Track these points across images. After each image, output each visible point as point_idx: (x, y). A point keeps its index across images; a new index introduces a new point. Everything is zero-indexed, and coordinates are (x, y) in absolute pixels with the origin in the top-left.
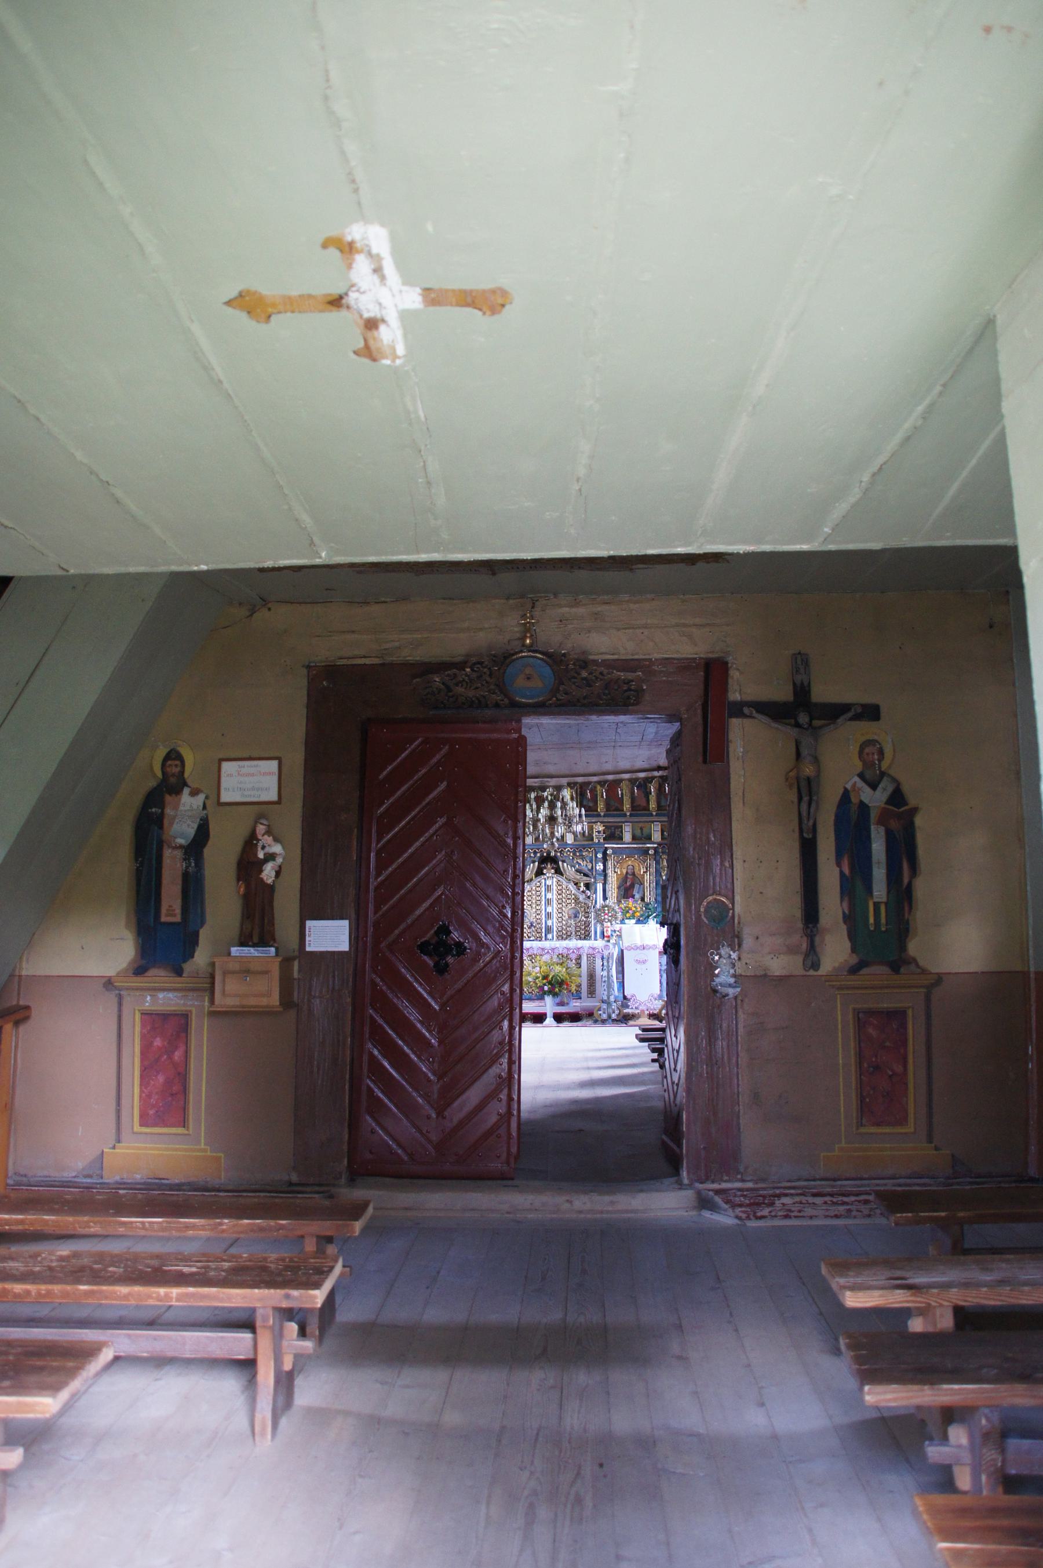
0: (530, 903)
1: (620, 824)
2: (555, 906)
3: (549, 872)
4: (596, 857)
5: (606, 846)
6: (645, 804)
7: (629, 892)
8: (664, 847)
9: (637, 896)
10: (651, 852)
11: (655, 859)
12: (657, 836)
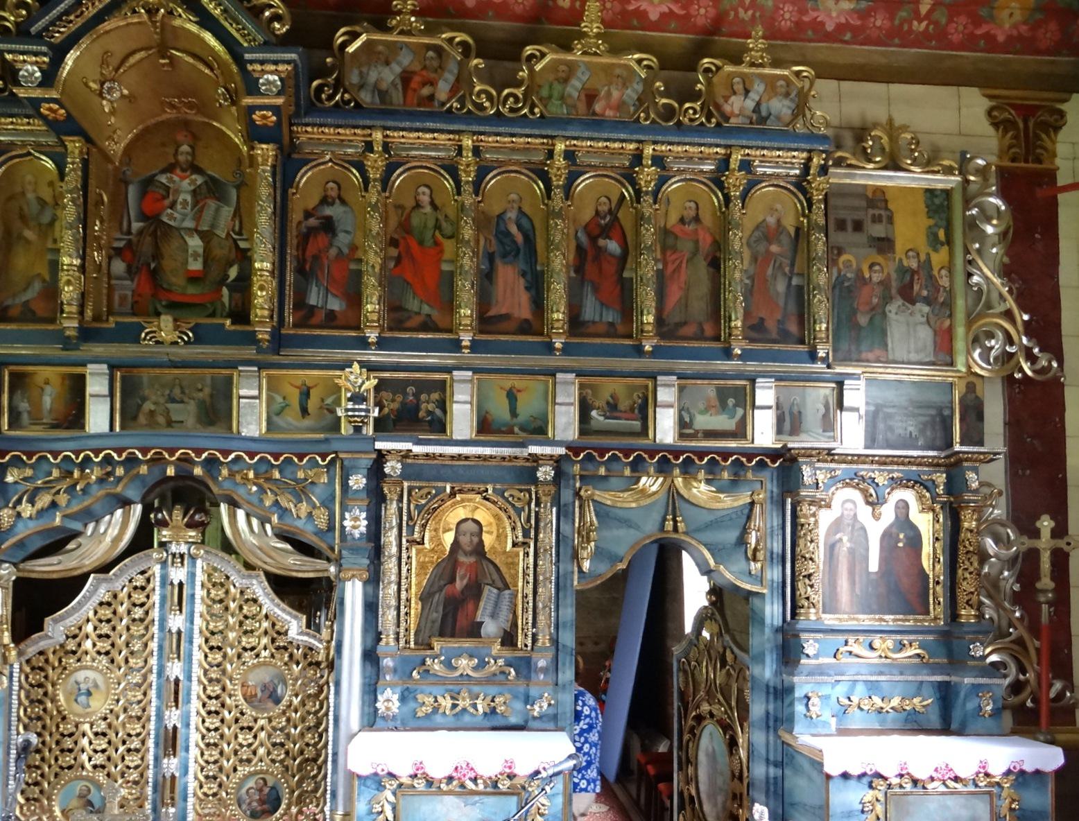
1: (437, 376)
2: (198, 656)
4: (345, 486)
6: (524, 311)
8: (589, 458)
9: (491, 628)
10: (545, 473)
11: (556, 501)
12: (565, 423)
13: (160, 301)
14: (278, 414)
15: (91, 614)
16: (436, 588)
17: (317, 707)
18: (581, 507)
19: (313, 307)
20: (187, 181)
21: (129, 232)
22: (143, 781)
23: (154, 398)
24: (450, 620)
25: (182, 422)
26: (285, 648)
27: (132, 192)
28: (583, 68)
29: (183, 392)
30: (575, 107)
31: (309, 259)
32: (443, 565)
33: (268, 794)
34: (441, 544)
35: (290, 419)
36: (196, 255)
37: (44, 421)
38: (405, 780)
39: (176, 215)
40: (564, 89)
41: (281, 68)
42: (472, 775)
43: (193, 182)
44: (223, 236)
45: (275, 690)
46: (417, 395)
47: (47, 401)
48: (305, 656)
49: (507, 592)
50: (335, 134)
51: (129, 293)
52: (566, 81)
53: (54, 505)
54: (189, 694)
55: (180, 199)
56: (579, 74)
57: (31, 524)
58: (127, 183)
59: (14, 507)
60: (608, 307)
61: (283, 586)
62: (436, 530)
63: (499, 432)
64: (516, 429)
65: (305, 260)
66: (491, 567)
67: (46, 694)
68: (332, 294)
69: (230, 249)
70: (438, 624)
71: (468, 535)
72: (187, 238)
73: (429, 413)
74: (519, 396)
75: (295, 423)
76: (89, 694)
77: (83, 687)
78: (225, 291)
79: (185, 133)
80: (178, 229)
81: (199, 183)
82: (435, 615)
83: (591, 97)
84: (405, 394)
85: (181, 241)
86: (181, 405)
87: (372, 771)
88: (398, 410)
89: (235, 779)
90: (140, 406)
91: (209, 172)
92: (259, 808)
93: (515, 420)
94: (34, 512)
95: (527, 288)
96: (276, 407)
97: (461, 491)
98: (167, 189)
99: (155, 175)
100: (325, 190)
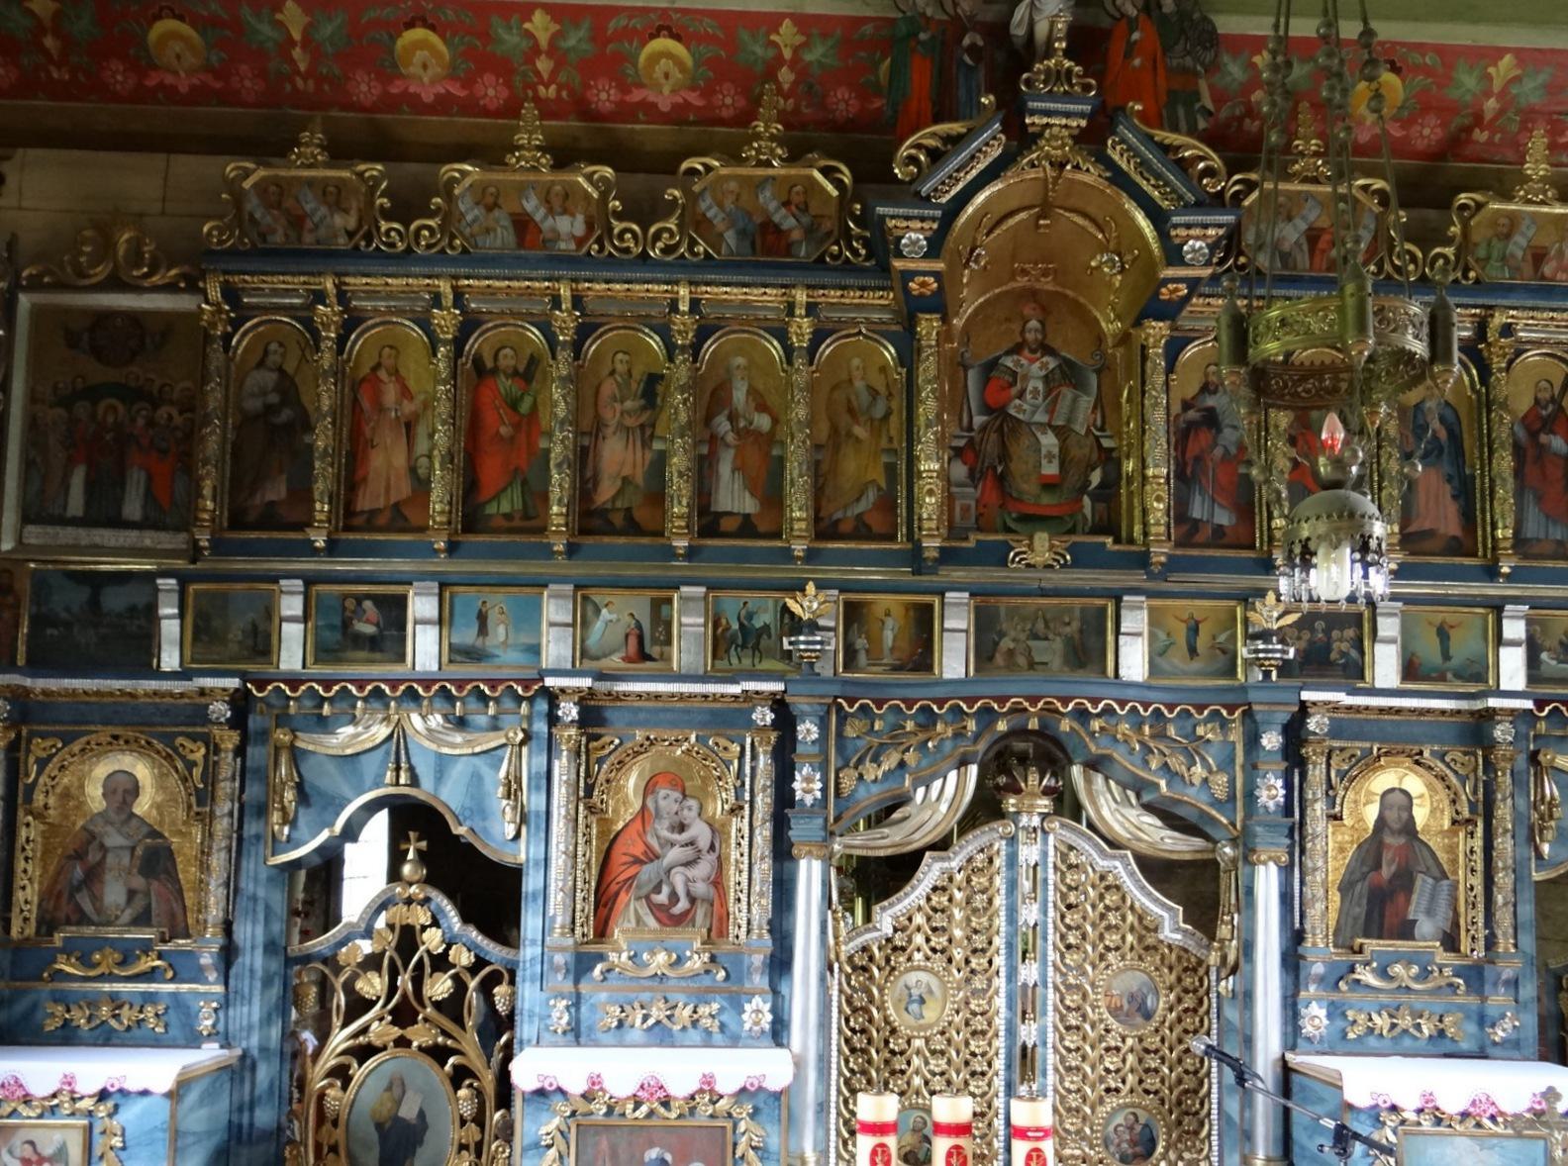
0: (943, 940)
3: (1031, 807)
5: (1306, 695)
7: (1389, 910)
9: (1425, 926)
13: (1010, 513)
14: (1161, 655)
15: (922, 902)
16: (1358, 875)
17: (1197, 1024)
18: (1535, 774)
19: (1196, 523)
20: (1037, 364)
21: (970, 428)
22: (991, 1113)
23: (1013, 633)
24: (1376, 915)
25: (1046, 664)
26: (1155, 948)
27: (973, 376)
28: (1527, 222)
29: (1047, 626)
30: (1518, 269)
31: (1190, 462)
32: (1366, 847)
33: (1141, 1133)
34: (1361, 820)
35: (1176, 661)
36: (1050, 457)
37: (885, 661)
38: (1411, 1116)
39: (1025, 407)
40: (1506, 247)
41: (1211, 232)
42: (1492, 1110)
43: (1044, 366)
44: (1083, 432)
45: (1144, 1002)
46: (1327, 632)
47: (888, 636)
48: (1179, 958)
49: (1445, 882)
50: (1203, 305)
51: (973, 503)
52: (1508, 236)
53: (902, 764)
54: (1045, 1004)
55: (1030, 388)
56: (1523, 228)
57: (875, 789)
58: (966, 368)
59: (856, 767)
60: (1555, 522)
61: (1157, 870)
62: (1355, 802)
63: (1426, 678)
64: (1449, 676)
65: (1185, 464)
66: (1425, 850)
67: (871, 1001)
68: (1221, 506)
69: (1092, 448)
70: (1362, 921)
71: (1395, 809)
72: (1039, 435)
73: (1343, 654)
74: (1453, 633)
75: (1181, 666)
76: (922, 1001)
77: (915, 992)
78: (1086, 500)
79: (1033, 305)
80: (1029, 424)
81: (1052, 366)
82: (1357, 910)
83: (1539, 257)
84: (1313, 630)
85: (1032, 439)
86: (1045, 643)
87: (1372, 1103)
88: (1305, 651)
89: (1102, 1111)
90: (996, 644)
91: (1063, 354)
92: (1130, 1151)
93: (1448, 664)
94: (880, 774)
95: (1455, 497)
96: (1160, 645)
97: (1387, 754)
98: (1015, 374)
99: (999, 357)
100: (1206, 375)
